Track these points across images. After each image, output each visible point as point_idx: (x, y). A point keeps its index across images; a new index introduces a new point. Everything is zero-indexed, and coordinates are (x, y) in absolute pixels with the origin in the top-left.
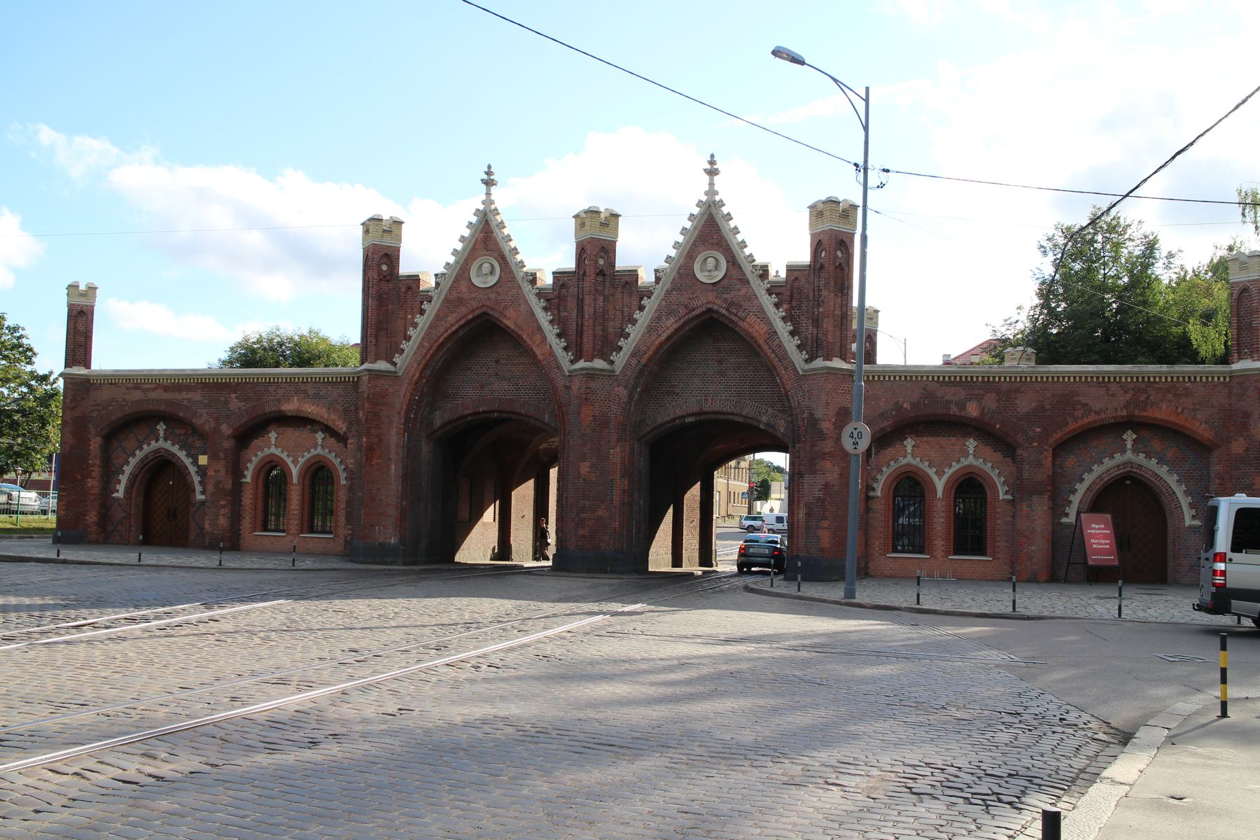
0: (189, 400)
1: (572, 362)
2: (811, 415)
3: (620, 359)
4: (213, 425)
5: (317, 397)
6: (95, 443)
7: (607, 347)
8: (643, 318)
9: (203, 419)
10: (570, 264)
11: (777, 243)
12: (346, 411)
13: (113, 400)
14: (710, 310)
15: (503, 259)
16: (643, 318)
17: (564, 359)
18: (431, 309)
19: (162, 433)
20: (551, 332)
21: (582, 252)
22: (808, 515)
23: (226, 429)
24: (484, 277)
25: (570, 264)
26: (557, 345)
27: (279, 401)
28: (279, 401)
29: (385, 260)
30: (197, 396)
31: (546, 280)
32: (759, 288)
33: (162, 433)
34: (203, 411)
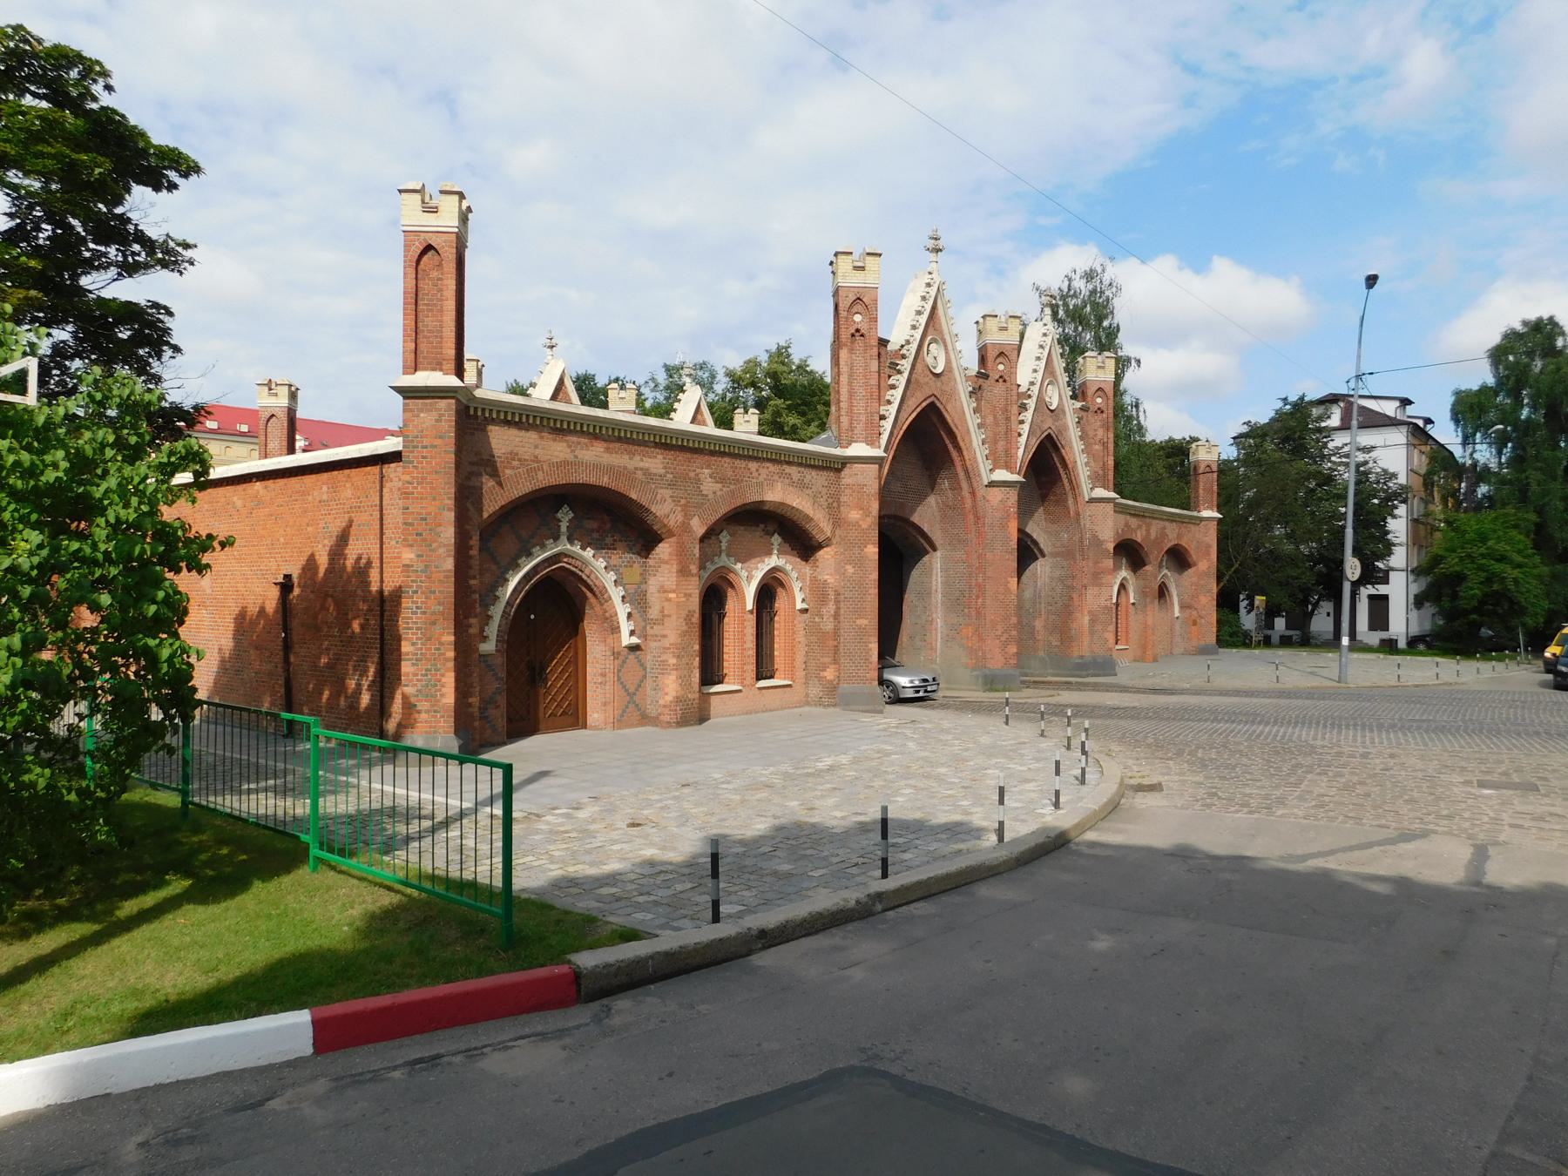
0: (646, 472)
2: (1095, 537)
4: (680, 518)
5: (802, 486)
6: (475, 541)
9: (664, 508)
12: (830, 507)
13: (513, 455)
19: (564, 526)
22: (1093, 621)
23: (699, 528)
27: (761, 485)
28: (761, 485)
30: (655, 462)
33: (564, 526)
34: (667, 493)
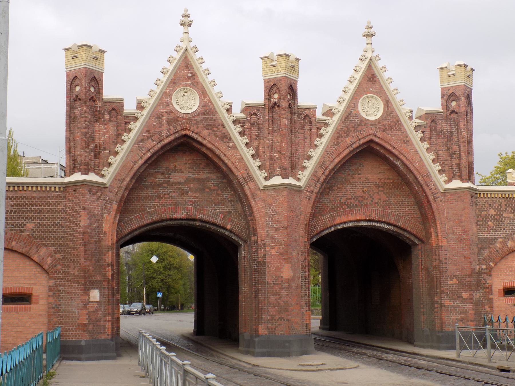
1: (266, 179)
3: (304, 177)
7: (292, 168)
8: (322, 143)
10: (258, 98)
11: (418, 94)
14: (371, 141)
15: (203, 92)
16: (322, 143)
17: (259, 176)
18: (136, 127)
20: (247, 153)
21: (271, 87)
24: (186, 104)
25: (258, 98)
26: (254, 164)
29: (93, 83)
31: (237, 112)
32: (409, 126)
